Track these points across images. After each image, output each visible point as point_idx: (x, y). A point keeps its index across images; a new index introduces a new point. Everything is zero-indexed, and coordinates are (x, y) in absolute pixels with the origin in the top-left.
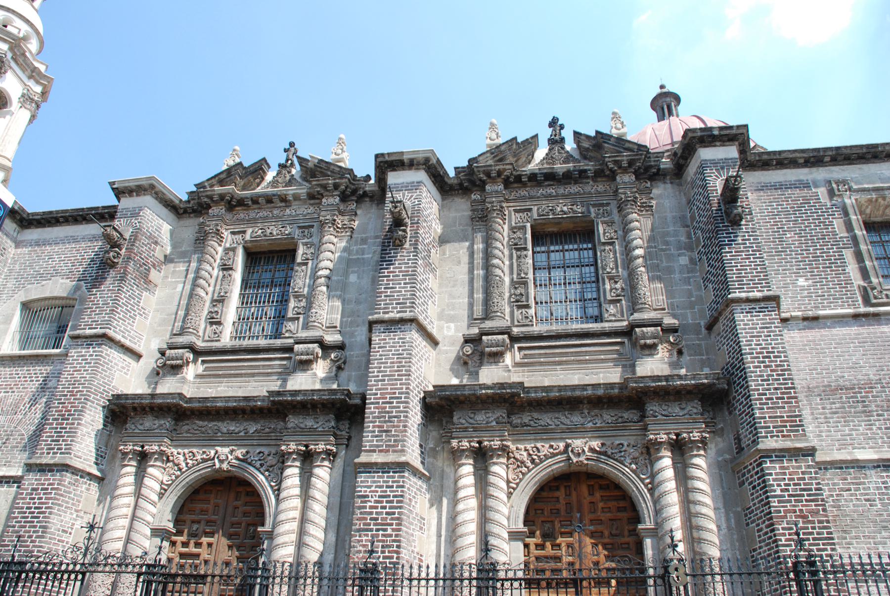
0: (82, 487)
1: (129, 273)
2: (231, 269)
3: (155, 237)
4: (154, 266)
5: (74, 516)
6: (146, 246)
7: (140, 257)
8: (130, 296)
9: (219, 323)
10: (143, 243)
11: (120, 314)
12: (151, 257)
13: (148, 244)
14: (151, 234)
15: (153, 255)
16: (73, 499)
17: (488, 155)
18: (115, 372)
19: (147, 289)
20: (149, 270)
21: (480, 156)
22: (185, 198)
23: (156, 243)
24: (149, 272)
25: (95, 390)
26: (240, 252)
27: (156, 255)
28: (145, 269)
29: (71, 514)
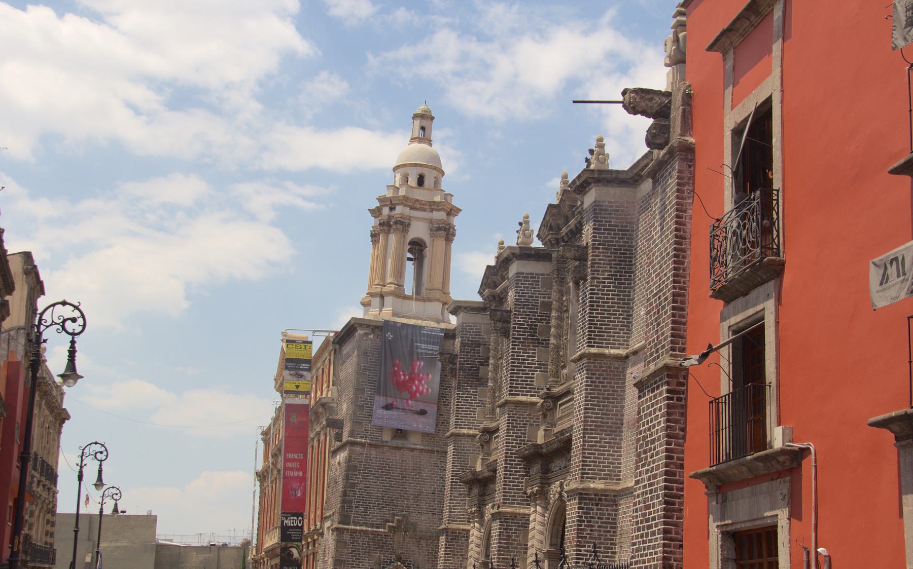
0: (461, 540)
3: (476, 341)
4: (482, 364)
5: (461, 559)
6: (470, 353)
7: (467, 364)
8: (466, 397)
10: (467, 352)
11: (462, 414)
12: (477, 359)
13: (471, 350)
14: (472, 341)
15: (479, 356)
16: (457, 549)
17: (543, 228)
18: (468, 456)
20: (478, 369)
21: (539, 231)
27: (481, 354)
28: (474, 370)
29: (458, 558)
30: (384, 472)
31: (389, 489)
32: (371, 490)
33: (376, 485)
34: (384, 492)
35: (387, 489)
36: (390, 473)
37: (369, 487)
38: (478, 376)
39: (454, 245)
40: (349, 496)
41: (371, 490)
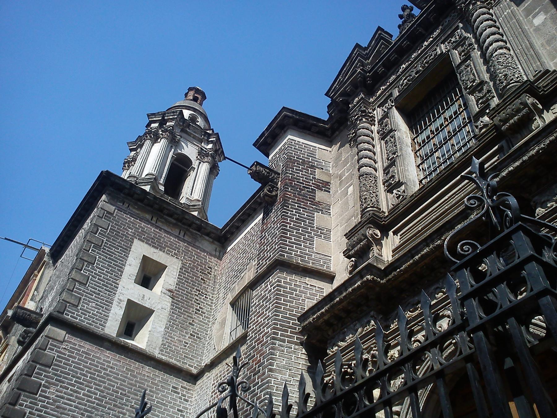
1: (290, 198)
2: (391, 131)
7: (297, 182)
9: (399, 184)
13: (303, 168)
15: (315, 178)
19: (318, 210)
20: (313, 191)
22: (325, 117)
23: (313, 167)
24: (315, 193)
25: (281, 325)
26: (395, 113)
27: (317, 177)
30: (96, 379)
31: (97, 410)
32: (65, 404)
33: (77, 397)
34: (87, 411)
35: (94, 408)
36: (105, 383)
37: (63, 398)
38: (314, 200)
39: (215, 181)
40: (22, 405)
41: (65, 404)
